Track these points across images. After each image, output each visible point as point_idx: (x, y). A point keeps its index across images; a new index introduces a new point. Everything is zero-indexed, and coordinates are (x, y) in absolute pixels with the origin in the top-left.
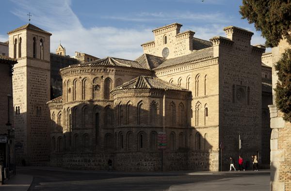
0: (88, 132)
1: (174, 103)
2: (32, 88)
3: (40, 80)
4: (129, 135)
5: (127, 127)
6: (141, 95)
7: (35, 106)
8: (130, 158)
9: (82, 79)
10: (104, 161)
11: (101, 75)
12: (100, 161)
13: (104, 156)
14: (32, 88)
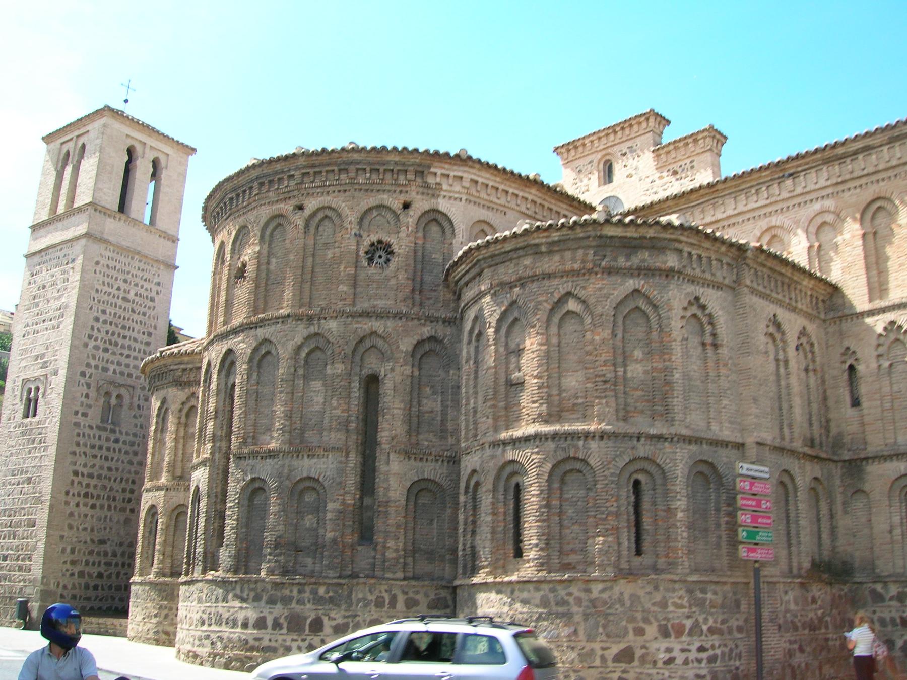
0: (321, 467)
1: (778, 326)
2: (97, 320)
3: (131, 296)
4: (563, 481)
5: (555, 436)
6: (635, 261)
7: (98, 390)
9: (307, 212)
11: (403, 198)
14: (97, 320)
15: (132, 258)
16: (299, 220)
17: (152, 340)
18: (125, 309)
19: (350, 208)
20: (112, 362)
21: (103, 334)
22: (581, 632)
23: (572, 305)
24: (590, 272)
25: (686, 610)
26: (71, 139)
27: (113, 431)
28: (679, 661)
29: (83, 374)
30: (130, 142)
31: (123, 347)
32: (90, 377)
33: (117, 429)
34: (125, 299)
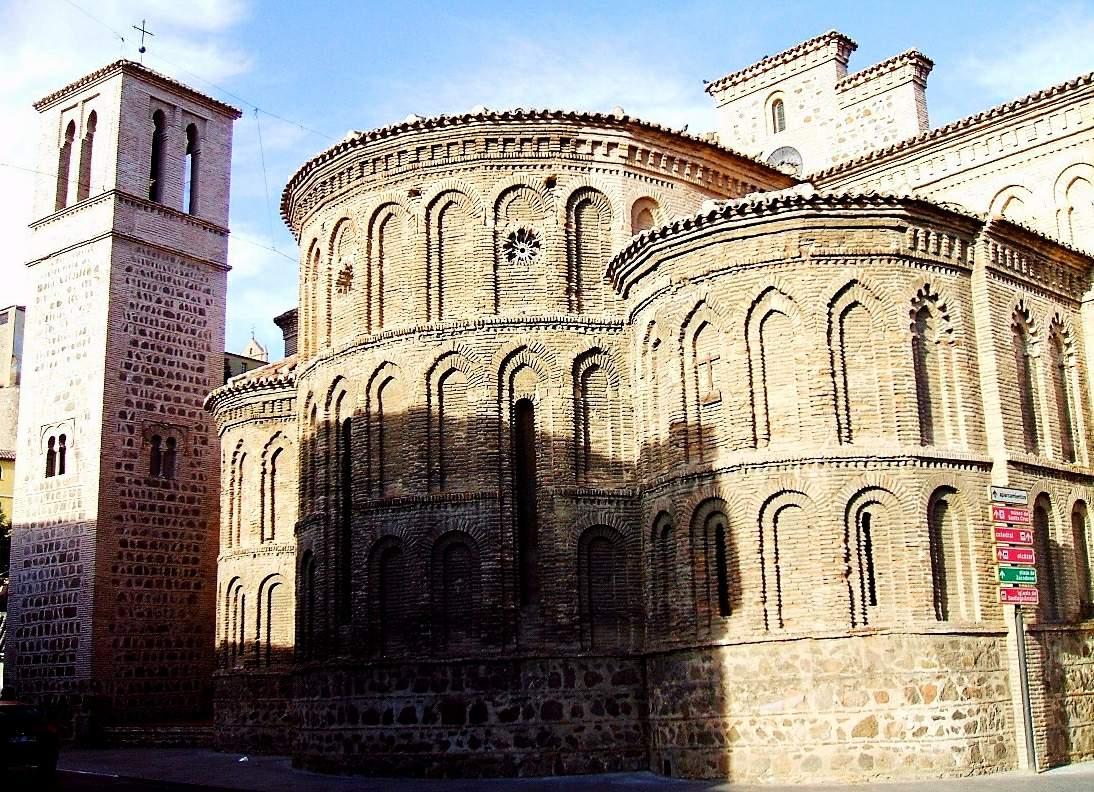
2: (135, 343)
3: (175, 310)
7: (144, 432)
8: (795, 680)
9: (426, 199)
10: (576, 712)
11: (546, 174)
12: (552, 711)
13: (579, 683)
14: (135, 343)
15: (173, 260)
16: (419, 207)
17: (206, 364)
18: (168, 328)
20: (159, 398)
21: (144, 361)
22: (811, 701)
23: (774, 301)
24: (798, 259)
25: (936, 670)
26: (76, 106)
27: (166, 486)
28: (933, 727)
29: (123, 415)
30: (155, 106)
31: (170, 376)
32: (132, 418)
33: (171, 482)
34: (168, 314)
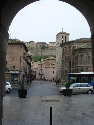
0: (66, 69)
16: (64, 48)
19: (67, 47)
23: (78, 56)
